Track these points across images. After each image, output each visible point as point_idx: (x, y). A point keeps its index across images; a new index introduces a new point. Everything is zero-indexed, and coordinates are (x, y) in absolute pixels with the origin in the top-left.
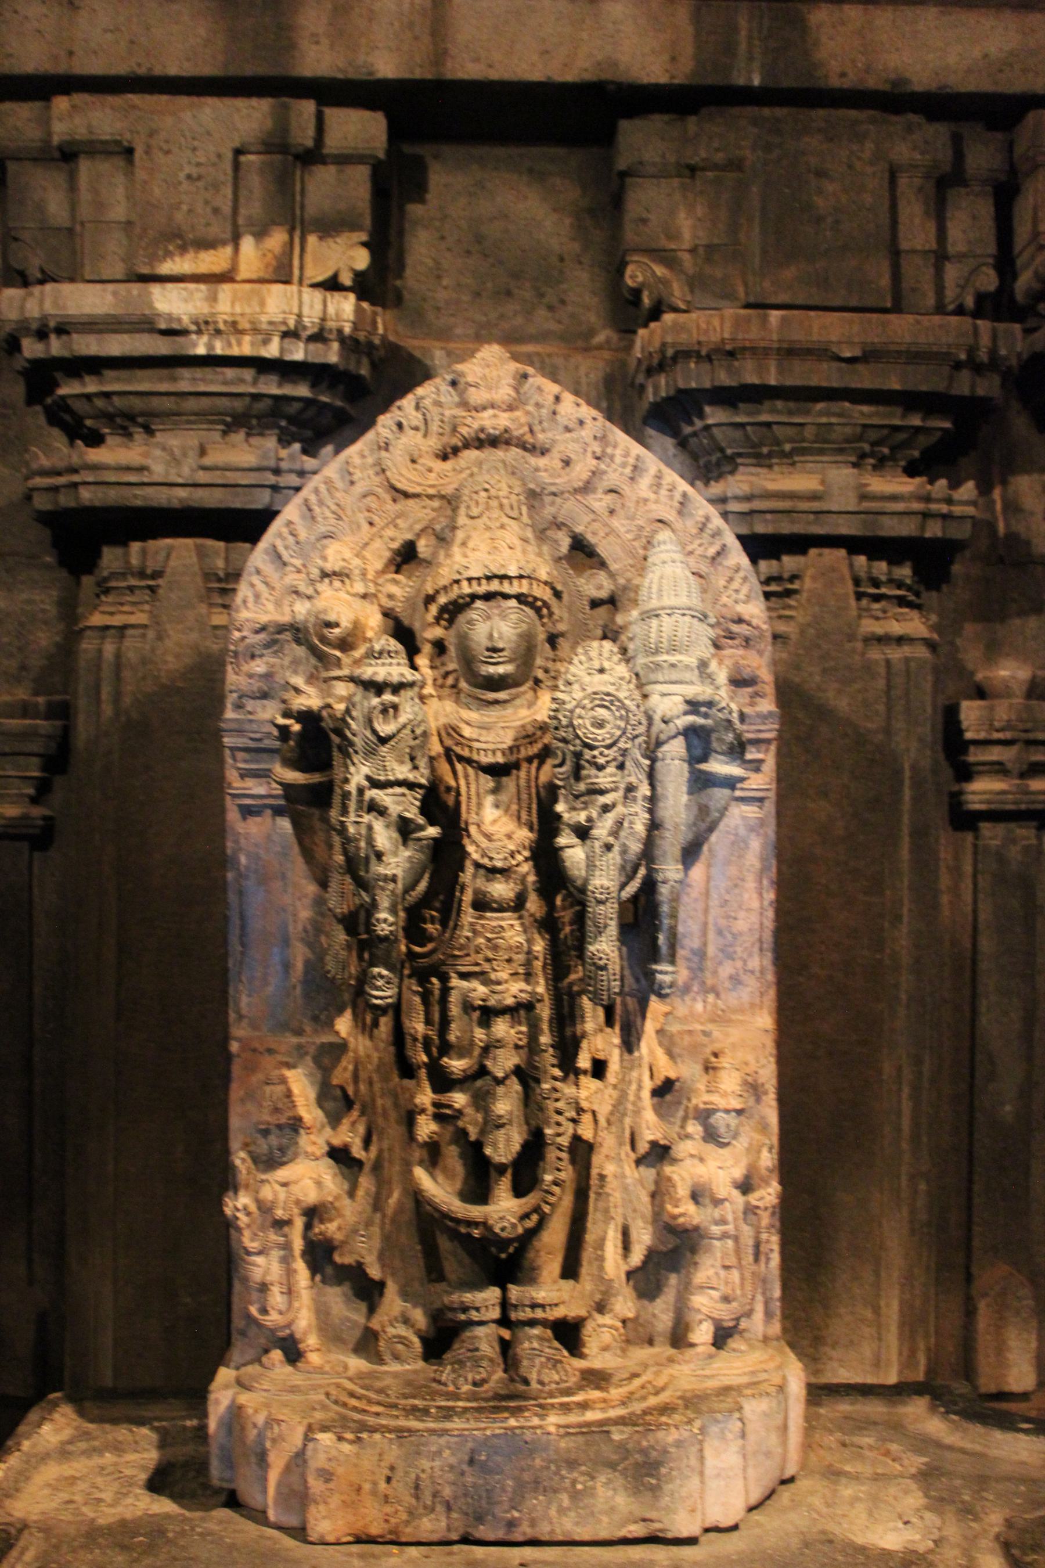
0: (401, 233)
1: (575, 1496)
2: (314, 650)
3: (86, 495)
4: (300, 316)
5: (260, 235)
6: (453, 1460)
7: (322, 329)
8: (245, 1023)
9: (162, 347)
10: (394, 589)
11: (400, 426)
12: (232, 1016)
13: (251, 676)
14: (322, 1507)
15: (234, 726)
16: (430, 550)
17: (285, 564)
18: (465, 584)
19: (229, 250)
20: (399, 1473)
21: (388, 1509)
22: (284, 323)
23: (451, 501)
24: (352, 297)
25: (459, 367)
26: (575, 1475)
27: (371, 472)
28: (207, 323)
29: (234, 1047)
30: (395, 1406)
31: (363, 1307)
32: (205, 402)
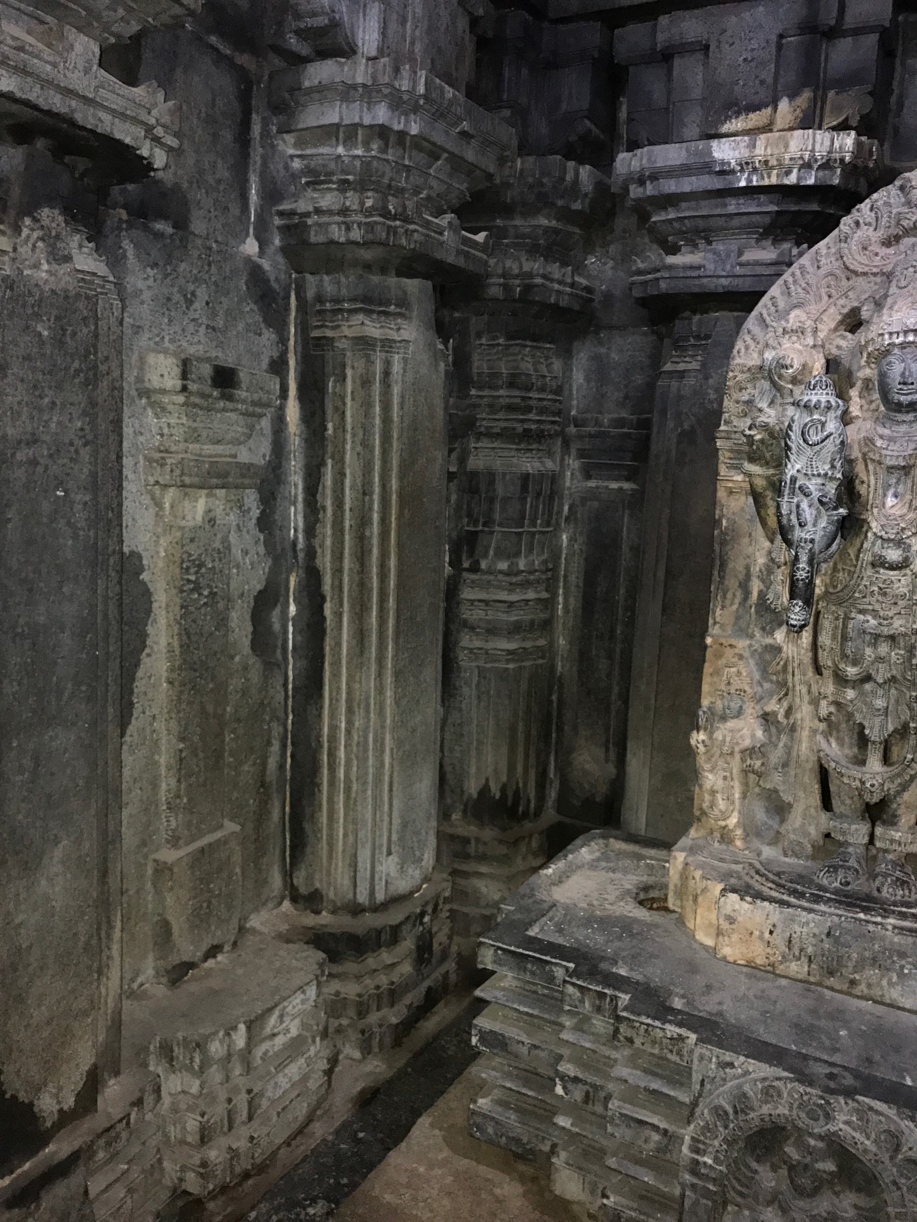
0: (902, 82)
1: (901, 975)
2: (774, 384)
3: (663, 285)
4: (813, 151)
5: (792, 96)
6: (816, 931)
7: (828, 161)
8: (717, 626)
9: (717, 183)
10: (843, 344)
11: (857, 223)
12: (711, 621)
13: (737, 402)
14: (726, 938)
15: (723, 435)
16: (869, 313)
17: (767, 326)
18: (887, 336)
19: (769, 109)
20: (777, 931)
21: (769, 950)
22: (801, 158)
23: (889, 276)
24: (853, 133)
25: (907, 175)
26: (903, 962)
27: (833, 259)
28: (747, 163)
29: (709, 640)
30: (783, 887)
31: (777, 818)
32: (745, 219)
